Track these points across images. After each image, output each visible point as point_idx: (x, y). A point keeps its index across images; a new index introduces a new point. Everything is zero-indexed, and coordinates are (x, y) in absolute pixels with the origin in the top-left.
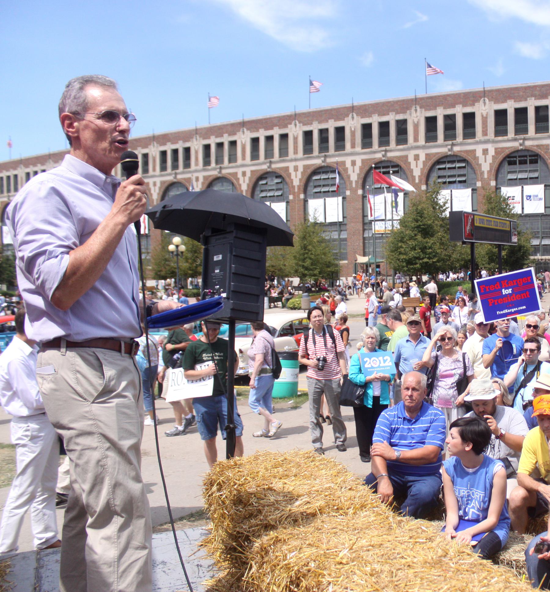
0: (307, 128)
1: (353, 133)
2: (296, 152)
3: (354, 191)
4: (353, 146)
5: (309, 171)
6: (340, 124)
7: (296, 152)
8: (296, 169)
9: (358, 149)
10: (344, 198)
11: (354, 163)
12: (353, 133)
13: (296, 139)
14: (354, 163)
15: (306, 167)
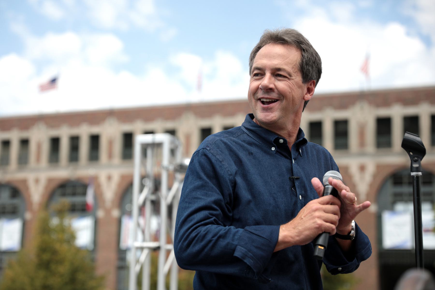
0: (54, 133)
1: (111, 143)
2: (38, 159)
3: (108, 212)
4: (110, 156)
5: (53, 185)
6: (95, 130)
7: (38, 159)
8: (37, 181)
9: (117, 159)
10: (97, 224)
11: (109, 178)
12: (111, 143)
13: (39, 146)
14: (109, 178)
15: (50, 180)
